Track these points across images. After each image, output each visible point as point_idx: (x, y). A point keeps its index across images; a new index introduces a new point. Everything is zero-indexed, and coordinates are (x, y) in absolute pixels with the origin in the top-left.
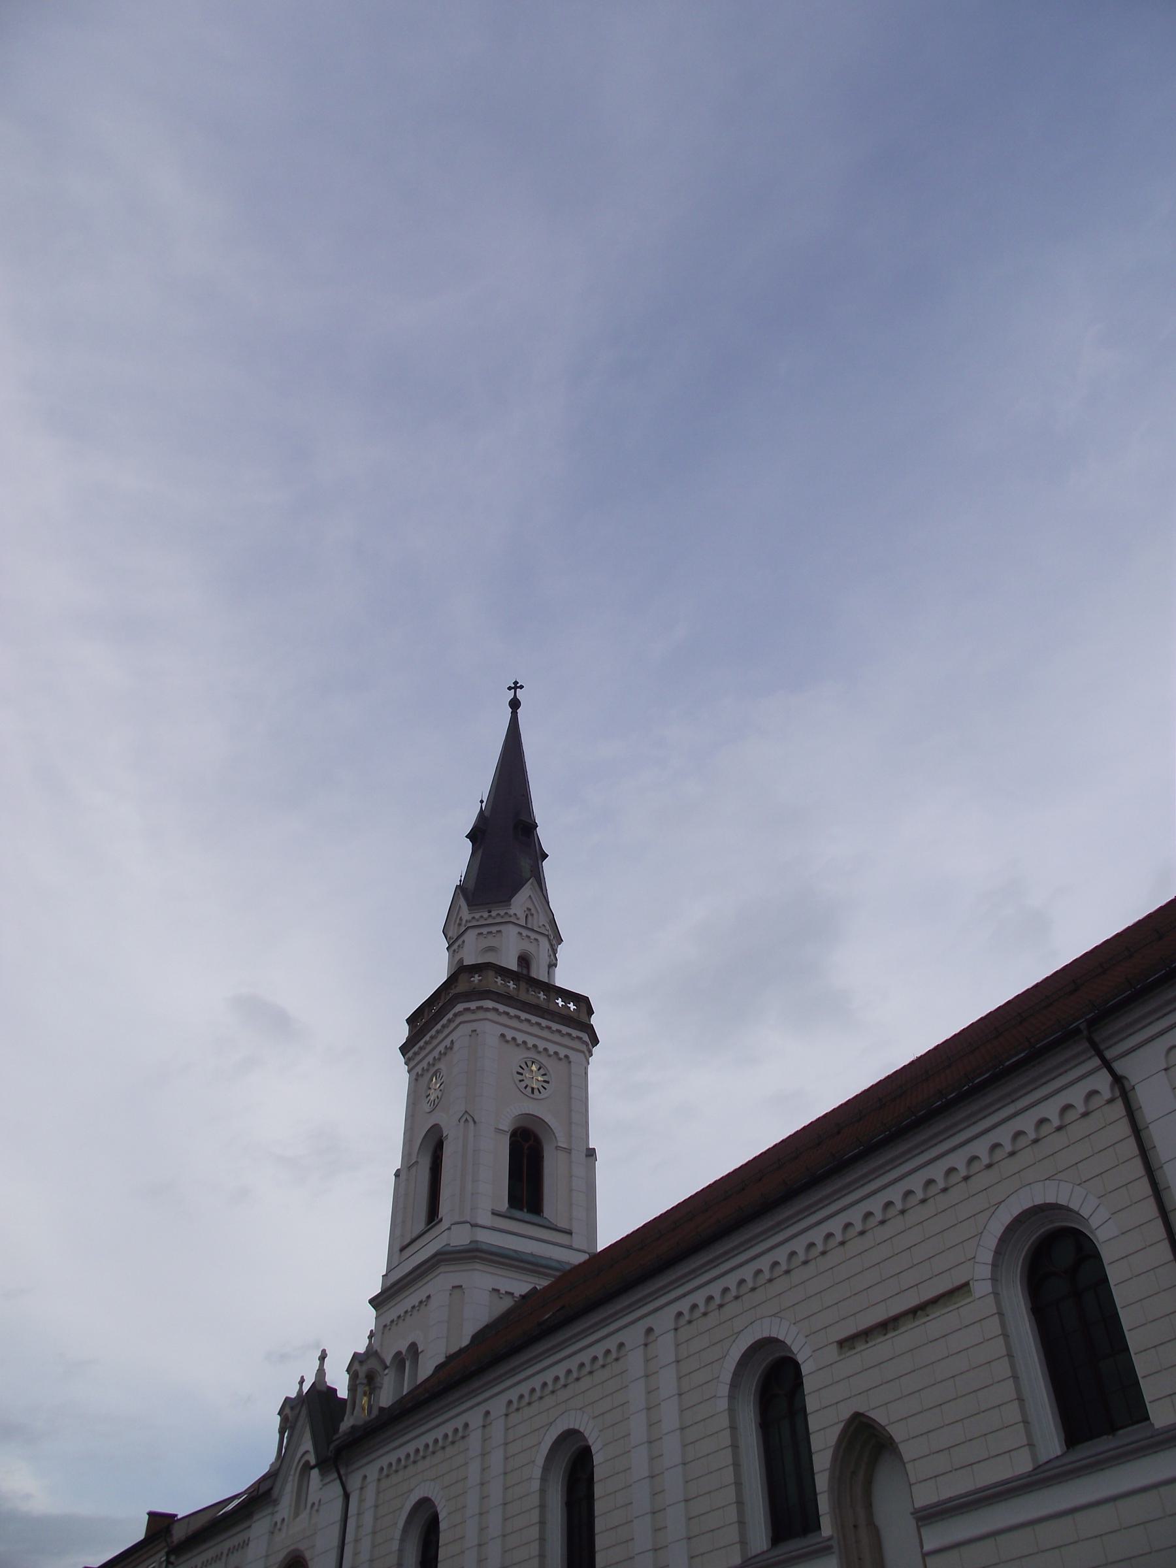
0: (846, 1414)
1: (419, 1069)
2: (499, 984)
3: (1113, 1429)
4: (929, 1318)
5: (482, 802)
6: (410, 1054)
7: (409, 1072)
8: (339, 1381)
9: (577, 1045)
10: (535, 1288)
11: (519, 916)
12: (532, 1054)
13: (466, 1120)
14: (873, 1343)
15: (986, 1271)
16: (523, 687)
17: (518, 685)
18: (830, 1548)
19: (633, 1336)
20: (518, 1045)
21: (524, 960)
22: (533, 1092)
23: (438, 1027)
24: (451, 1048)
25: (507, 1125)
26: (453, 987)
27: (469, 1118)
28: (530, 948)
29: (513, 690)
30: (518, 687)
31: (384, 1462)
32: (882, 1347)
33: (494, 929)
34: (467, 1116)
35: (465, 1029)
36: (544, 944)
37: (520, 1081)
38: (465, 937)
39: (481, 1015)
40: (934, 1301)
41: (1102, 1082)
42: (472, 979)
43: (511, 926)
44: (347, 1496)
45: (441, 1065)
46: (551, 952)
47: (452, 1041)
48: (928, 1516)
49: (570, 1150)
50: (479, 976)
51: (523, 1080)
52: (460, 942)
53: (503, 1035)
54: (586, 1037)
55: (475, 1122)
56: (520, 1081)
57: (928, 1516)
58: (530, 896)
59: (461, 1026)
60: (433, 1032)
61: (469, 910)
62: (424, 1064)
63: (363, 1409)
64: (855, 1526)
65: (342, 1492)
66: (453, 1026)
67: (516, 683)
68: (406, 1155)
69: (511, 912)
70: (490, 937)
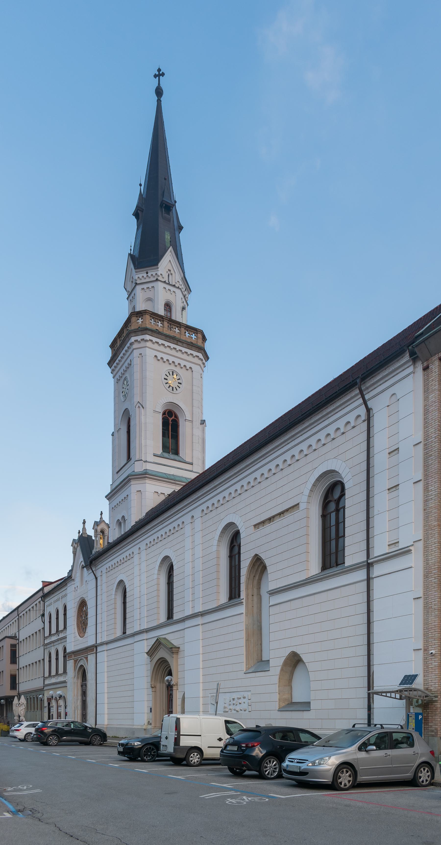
2: (153, 324)
9: (196, 360)
11: (163, 276)
12: (172, 367)
13: (139, 407)
20: (164, 362)
22: (173, 390)
28: (171, 298)
34: (139, 404)
36: (179, 294)
37: (166, 383)
39: (143, 344)
42: (138, 321)
46: (183, 300)
49: (192, 421)
50: (141, 319)
53: (156, 356)
56: (166, 383)
58: (170, 261)
67: (159, 70)
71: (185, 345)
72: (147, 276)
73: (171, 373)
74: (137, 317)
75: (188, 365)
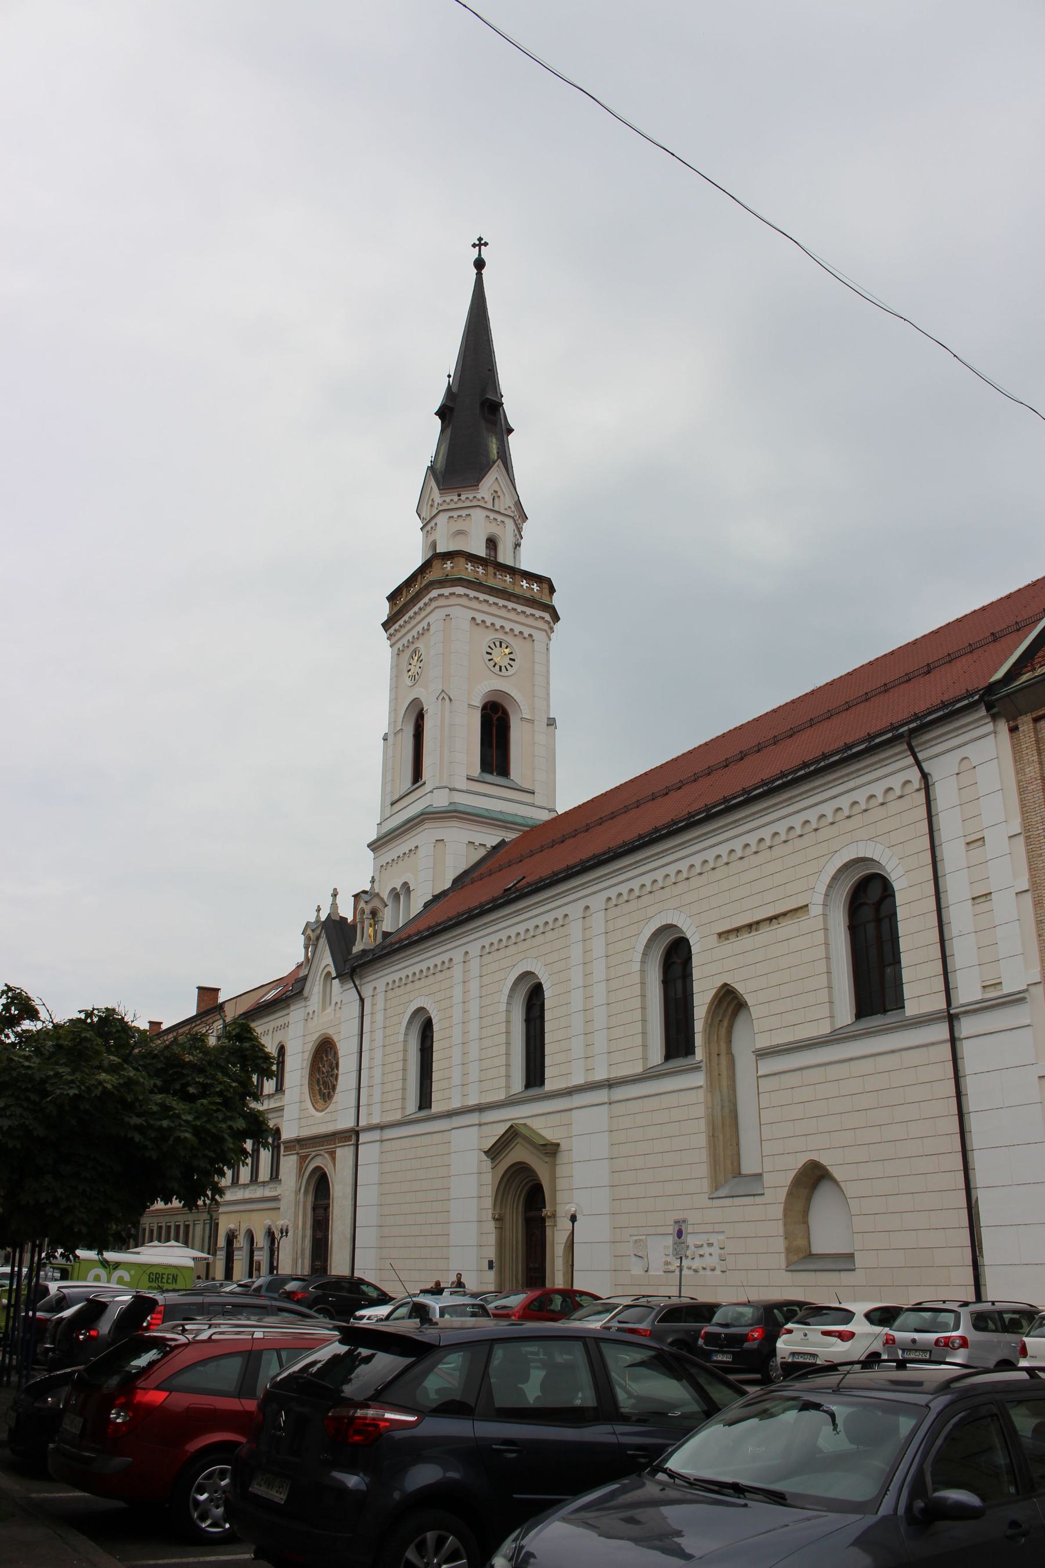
0: (719, 984)
1: (400, 645)
2: (469, 570)
3: (885, 1011)
4: (779, 926)
5: (449, 376)
6: (391, 631)
7: (391, 646)
8: (346, 911)
10: (503, 840)
12: (500, 636)
13: (443, 698)
14: (741, 938)
15: (819, 898)
16: (488, 244)
17: (483, 242)
18: (700, 1067)
19: (575, 910)
20: (487, 627)
21: (492, 543)
22: (500, 670)
23: (416, 609)
24: (428, 630)
25: (478, 703)
26: (428, 572)
27: (447, 698)
29: (477, 248)
30: (483, 244)
31: (389, 979)
32: (747, 941)
33: (463, 513)
34: (443, 695)
35: (440, 614)
36: (510, 524)
37: (490, 660)
38: (438, 519)
39: (453, 600)
40: (784, 914)
41: (915, 775)
42: (445, 566)
43: (478, 511)
44: (362, 1000)
45: (419, 644)
46: (516, 532)
47: (429, 623)
48: (762, 1054)
51: (492, 659)
52: (432, 524)
53: (473, 619)
54: (547, 616)
55: (450, 700)
56: (490, 660)
57: (762, 1054)
59: (437, 610)
60: (411, 613)
61: (440, 494)
62: (404, 641)
63: (370, 937)
64: (718, 1055)
65: (358, 997)
66: (429, 609)
67: (480, 239)
68: (392, 722)
69: (479, 496)
70: (460, 520)
71: (521, 601)
72: (460, 499)
73: (498, 644)
74: (443, 560)
75: (527, 632)
